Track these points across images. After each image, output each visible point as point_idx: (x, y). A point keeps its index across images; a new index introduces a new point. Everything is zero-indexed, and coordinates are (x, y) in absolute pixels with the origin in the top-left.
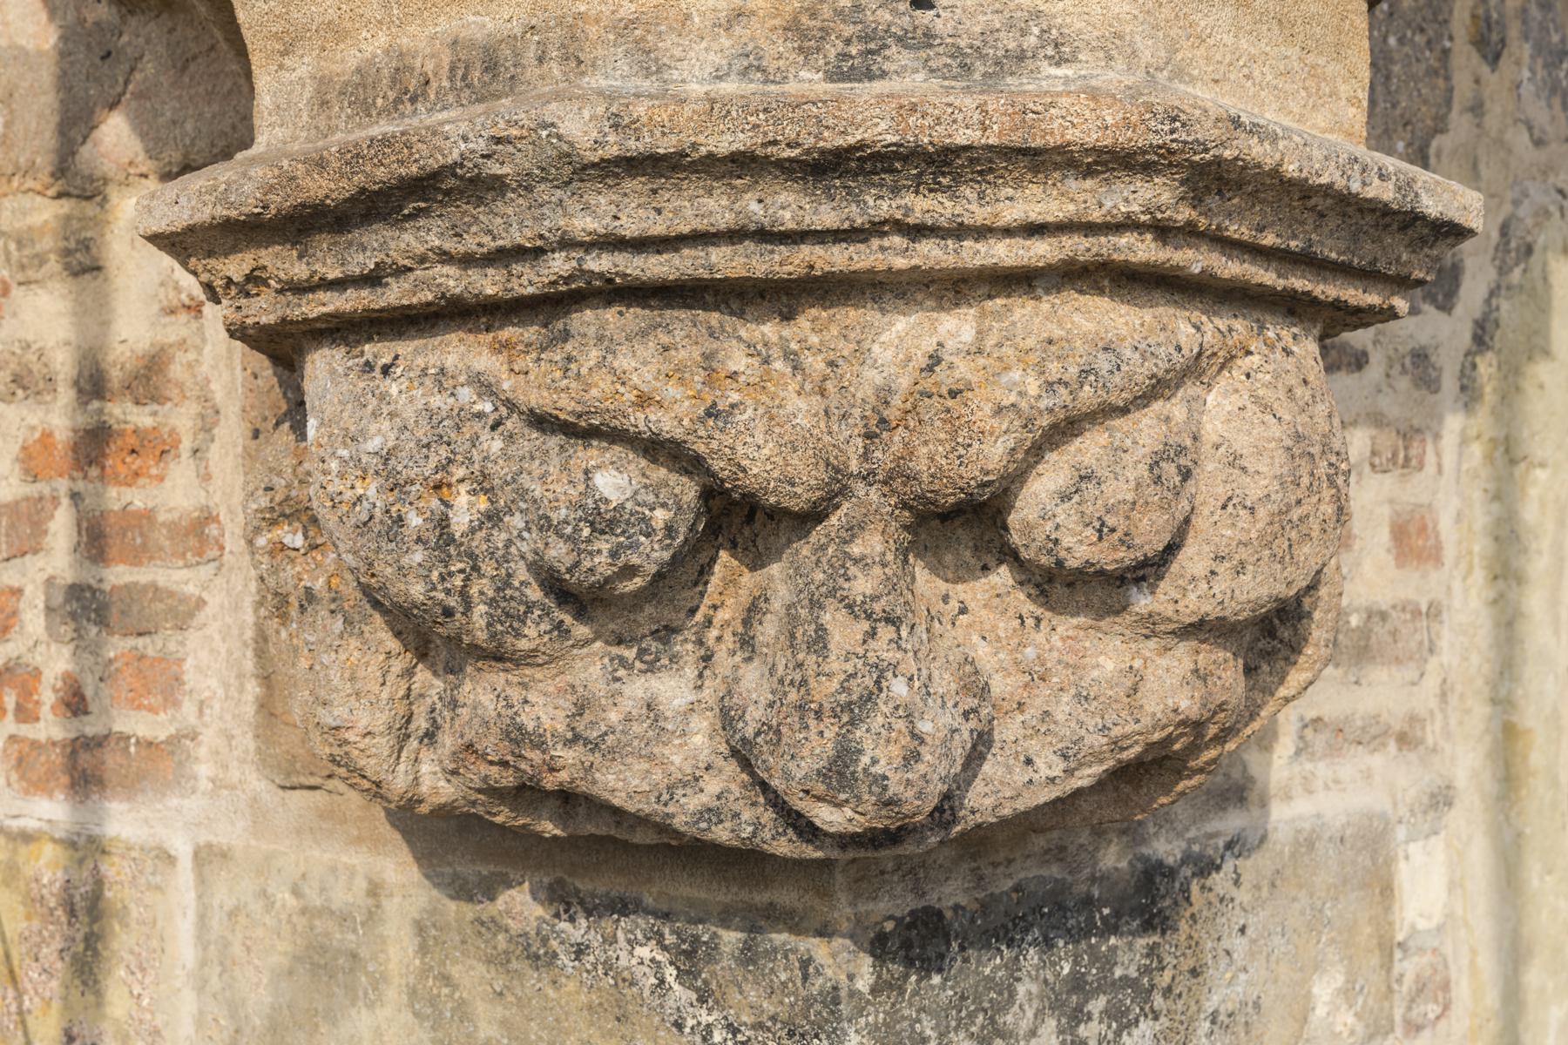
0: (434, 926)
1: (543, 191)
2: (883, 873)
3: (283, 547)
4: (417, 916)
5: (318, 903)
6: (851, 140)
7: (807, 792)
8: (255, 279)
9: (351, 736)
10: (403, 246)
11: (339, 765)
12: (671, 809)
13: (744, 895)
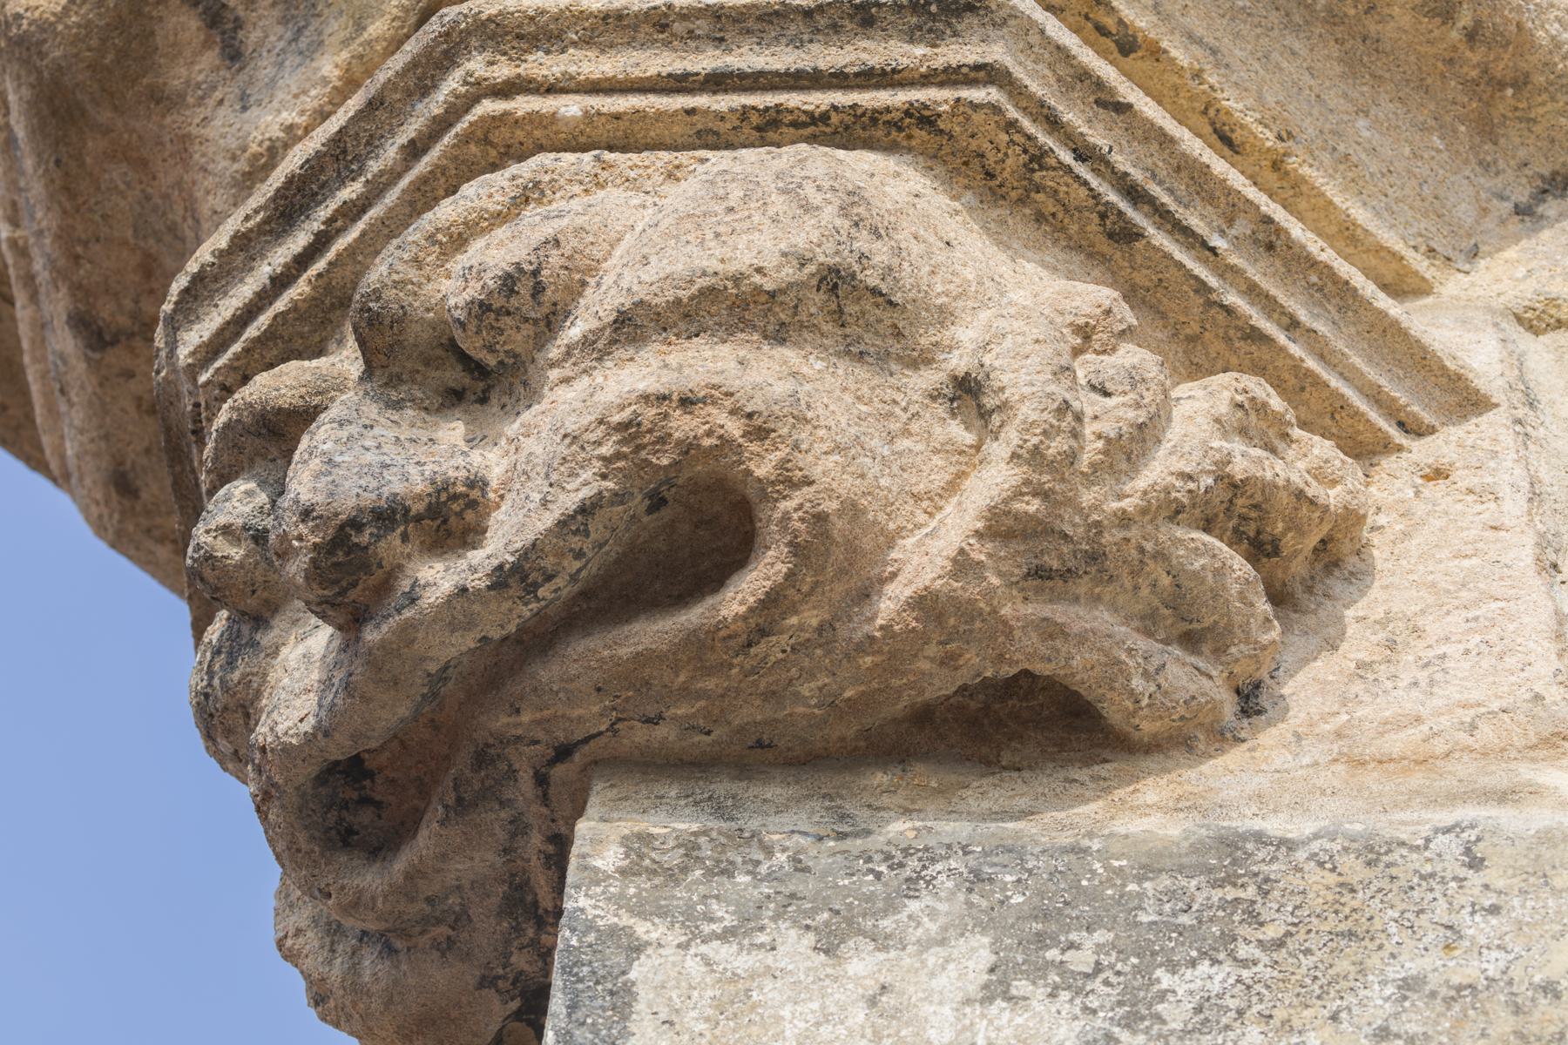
2: (662, 797)
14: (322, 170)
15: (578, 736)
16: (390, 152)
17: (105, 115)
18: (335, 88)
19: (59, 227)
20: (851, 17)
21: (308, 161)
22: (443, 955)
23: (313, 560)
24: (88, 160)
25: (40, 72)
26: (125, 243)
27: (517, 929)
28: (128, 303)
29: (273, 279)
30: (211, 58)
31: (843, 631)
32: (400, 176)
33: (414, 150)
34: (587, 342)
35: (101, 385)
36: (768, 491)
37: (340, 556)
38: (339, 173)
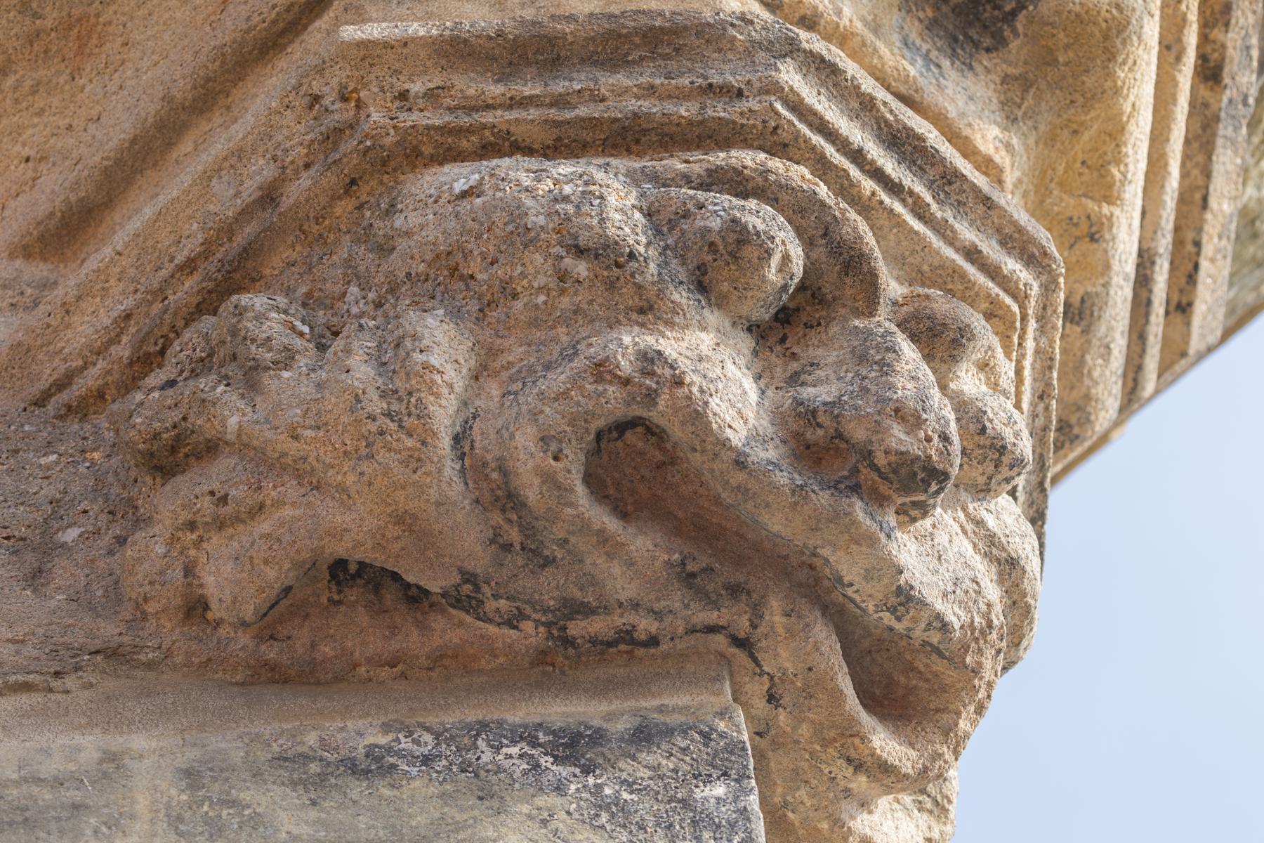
0: (211, 770)
1: (761, 55)
3: (293, 328)
4: (184, 766)
5: (15, 776)
6: (921, 131)
7: (897, 411)
8: (432, 96)
9: (438, 378)
10: (611, 81)
11: (393, 421)
12: (747, 450)
13: (632, 703)
14: (933, 165)
15: (759, 656)
16: (967, 234)
18: (838, 25)
20: (1037, 511)
21: (936, 150)
22: (492, 541)
23: (918, 458)
27: (545, 611)
29: (860, 151)
31: (845, 805)
32: (951, 244)
33: (972, 254)
34: (991, 539)
36: (947, 732)
37: (921, 475)
38: (935, 181)
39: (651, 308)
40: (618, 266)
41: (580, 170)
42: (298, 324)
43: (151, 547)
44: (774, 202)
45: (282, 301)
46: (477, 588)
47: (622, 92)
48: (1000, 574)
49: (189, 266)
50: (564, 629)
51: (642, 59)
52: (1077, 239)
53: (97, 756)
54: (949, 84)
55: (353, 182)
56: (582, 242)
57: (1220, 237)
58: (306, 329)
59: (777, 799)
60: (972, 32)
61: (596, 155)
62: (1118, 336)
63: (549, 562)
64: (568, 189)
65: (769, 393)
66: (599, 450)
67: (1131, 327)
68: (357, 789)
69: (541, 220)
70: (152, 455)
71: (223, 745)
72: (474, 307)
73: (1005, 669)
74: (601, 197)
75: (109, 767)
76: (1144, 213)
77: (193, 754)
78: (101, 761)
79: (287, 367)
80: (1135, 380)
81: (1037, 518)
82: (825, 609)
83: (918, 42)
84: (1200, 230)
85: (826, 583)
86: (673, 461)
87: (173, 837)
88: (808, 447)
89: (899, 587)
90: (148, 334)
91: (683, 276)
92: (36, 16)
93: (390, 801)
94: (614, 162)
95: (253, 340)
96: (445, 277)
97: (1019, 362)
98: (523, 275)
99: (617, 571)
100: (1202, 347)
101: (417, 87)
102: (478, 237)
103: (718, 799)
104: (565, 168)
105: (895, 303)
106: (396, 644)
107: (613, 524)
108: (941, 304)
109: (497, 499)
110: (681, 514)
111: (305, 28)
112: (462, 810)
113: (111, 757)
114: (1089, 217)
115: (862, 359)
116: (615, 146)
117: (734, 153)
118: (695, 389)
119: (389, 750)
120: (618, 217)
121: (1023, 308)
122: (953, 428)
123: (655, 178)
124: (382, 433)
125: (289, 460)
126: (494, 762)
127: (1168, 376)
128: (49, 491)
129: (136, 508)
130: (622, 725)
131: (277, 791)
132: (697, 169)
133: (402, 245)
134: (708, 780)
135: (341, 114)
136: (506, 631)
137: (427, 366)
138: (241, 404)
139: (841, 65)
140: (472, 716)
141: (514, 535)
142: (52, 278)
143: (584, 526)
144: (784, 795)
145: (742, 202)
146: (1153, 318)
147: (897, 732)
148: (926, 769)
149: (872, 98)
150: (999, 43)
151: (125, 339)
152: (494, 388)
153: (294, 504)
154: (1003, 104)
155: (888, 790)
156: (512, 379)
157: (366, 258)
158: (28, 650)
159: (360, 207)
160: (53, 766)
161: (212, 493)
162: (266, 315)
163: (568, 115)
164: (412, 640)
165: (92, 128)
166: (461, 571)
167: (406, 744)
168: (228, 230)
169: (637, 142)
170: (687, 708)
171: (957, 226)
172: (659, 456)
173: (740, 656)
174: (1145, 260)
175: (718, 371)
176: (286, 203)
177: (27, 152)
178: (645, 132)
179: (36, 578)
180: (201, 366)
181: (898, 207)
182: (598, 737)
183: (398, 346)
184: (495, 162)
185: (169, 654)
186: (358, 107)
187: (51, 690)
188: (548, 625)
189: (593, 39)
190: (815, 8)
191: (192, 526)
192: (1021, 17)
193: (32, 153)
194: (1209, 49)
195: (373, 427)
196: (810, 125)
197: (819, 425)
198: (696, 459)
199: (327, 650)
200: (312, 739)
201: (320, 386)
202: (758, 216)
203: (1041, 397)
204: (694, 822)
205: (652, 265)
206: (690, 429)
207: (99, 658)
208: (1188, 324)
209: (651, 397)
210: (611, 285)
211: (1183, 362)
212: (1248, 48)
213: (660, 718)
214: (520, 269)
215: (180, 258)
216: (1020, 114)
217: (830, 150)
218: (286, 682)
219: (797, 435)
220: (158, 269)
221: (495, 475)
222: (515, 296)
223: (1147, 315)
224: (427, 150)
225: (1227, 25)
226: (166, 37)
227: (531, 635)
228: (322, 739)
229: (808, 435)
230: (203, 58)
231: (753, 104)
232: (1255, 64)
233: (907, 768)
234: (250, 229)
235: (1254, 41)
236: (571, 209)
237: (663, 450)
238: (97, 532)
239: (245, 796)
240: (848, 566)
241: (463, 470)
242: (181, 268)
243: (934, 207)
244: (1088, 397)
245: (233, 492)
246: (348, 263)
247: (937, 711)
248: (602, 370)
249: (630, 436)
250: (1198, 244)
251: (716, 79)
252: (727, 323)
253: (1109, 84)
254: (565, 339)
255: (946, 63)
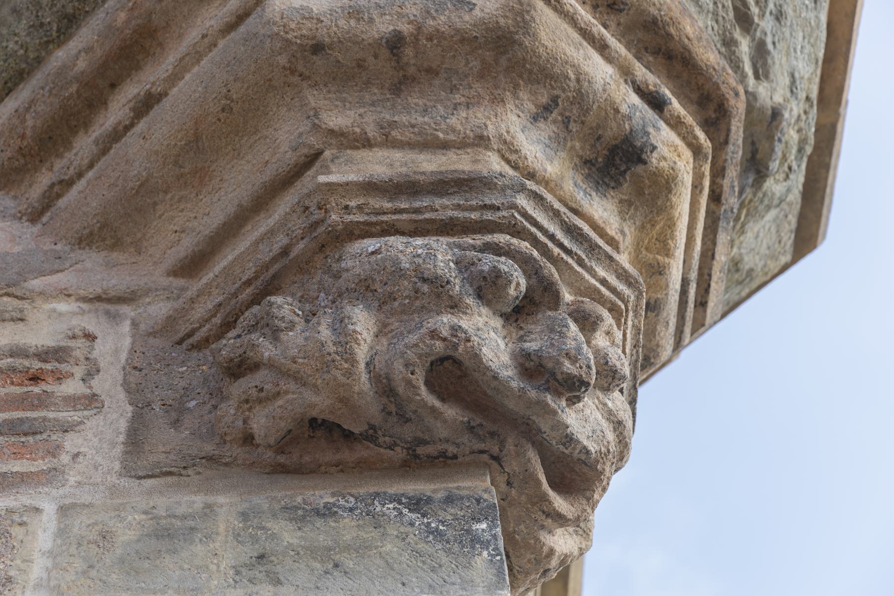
3: (295, 312)
5: (164, 514)
7: (567, 354)
8: (360, 208)
9: (359, 337)
13: (445, 485)
15: (503, 464)
16: (601, 272)
17: (503, 61)
19: (443, 32)
22: (383, 411)
23: (576, 376)
24: (480, 51)
25: (517, 33)
26: (442, 63)
28: (412, 61)
30: (534, 109)
32: (594, 277)
33: (604, 282)
35: (369, 44)
39: (456, 306)
40: (442, 287)
41: (426, 242)
42: (297, 310)
43: (228, 410)
44: (513, 258)
45: (290, 299)
46: (376, 432)
47: (445, 207)
48: (614, 428)
49: (248, 283)
50: (415, 450)
51: (455, 192)
52: (653, 274)
53: (202, 505)
54: (595, 203)
55: (323, 246)
56: (426, 276)
57: (720, 272)
58: (300, 313)
59: (511, 529)
60: (606, 180)
61: (433, 235)
62: (672, 317)
63: (408, 420)
64: (420, 251)
65: (510, 345)
66: (432, 370)
67: (678, 313)
68: (319, 522)
69: (407, 266)
70: (230, 368)
71: (259, 501)
72: (376, 304)
73: (616, 471)
74: (435, 256)
75: (208, 511)
76: (684, 262)
77: (246, 505)
78: (203, 509)
79: (291, 330)
80: (680, 338)
81: (633, 402)
82: (533, 443)
83: (581, 184)
84: (711, 269)
85: (534, 432)
86: (465, 375)
87: (236, 543)
88: (526, 370)
89: (567, 435)
90: (229, 313)
91: (471, 292)
92: (181, 167)
93: (334, 528)
94: (441, 239)
95: (276, 318)
96: (364, 289)
97: (624, 331)
98: (399, 290)
99: (439, 425)
100: (712, 322)
101: (353, 204)
102: (379, 272)
103: (483, 530)
104: (419, 241)
105: (568, 304)
106: (338, 457)
107: (437, 404)
108: (589, 305)
109: (385, 392)
110: (468, 399)
111: (303, 174)
112: (367, 533)
113: (208, 506)
114: (659, 264)
115: (552, 330)
116: (442, 232)
117: (495, 235)
118: (475, 343)
119: (334, 505)
120: (442, 264)
121: (626, 306)
122: (592, 362)
123: (459, 246)
124: (334, 361)
125: (291, 373)
126: (381, 511)
127: (696, 335)
128: (183, 384)
129: (222, 392)
130: (440, 495)
131: (283, 523)
132: (478, 243)
133: (345, 275)
134: (479, 521)
135: (318, 215)
136: (388, 451)
137: (354, 331)
138: (270, 347)
139: (545, 196)
140: (372, 490)
141: (393, 408)
142: (187, 285)
143: (424, 404)
144: (514, 527)
145: (499, 258)
146: (688, 309)
147: (565, 499)
148: (579, 516)
149: (559, 211)
150: (619, 184)
151: (218, 315)
152: (384, 341)
153: (293, 393)
154: (620, 212)
155: (561, 526)
156: (393, 337)
157: (328, 280)
158: (172, 457)
159: (326, 257)
160: (181, 510)
161: (256, 387)
162: (283, 305)
163: (421, 217)
164: (346, 455)
165: (205, 218)
166: (368, 424)
167: (342, 502)
168: (266, 267)
169: (452, 230)
170: (470, 488)
171: (597, 269)
172: (459, 373)
173: (495, 464)
174: (685, 283)
175: (486, 335)
176: (292, 255)
177: (176, 228)
178: (455, 225)
179: (176, 423)
180: (252, 329)
181: (570, 261)
182: (429, 500)
183: (341, 321)
184: (387, 238)
185: (236, 459)
186: (326, 212)
187: (181, 475)
188: (408, 449)
189: (432, 183)
190: (534, 169)
191: (247, 401)
192: (628, 173)
193: (178, 229)
194: (715, 187)
195: (329, 358)
196: (530, 223)
197: (532, 360)
198: (476, 374)
199: (307, 458)
200: (299, 499)
201: (306, 339)
202: (505, 265)
203: (635, 347)
204: (472, 540)
205: (457, 287)
206: (473, 361)
207: (204, 461)
208: (705, 311)
209: (455, 347)
210: (438, 296)
211: (703, 329)
212: (733, 187)
213: (457, 492)
214: (397, 287)
215: (244, 279)
216: (627, 217)
217: (539, 235)
218: (288, 473)
219: (521, 365)
220: (234, 284)
221: (384, 381)
222: (395, 300)
223: (686, 308)
224: (357, 232)
225: (724, 176)
226: (240, 177)
227: (399, 454)
228: (304, 499)
229: (526, 364)
230: (256, 188)
231: (505, 213)
232: (736, 194)
233: (570, 516)
234: (277, 267)
235: (736, 184)
236: (421, 261)
237: (461, 370)
238: (204, 403)
239: (269, 525)
240: (544, 425)
241: (370, 378)
242: (244, 283)
243: (587, 260)
244: (658, 346)
245: (266, 387)
246: (320, 282)
247: (584, 490)
248: (434, 334)
249: (446, 364)
250: (710, 275)
251: (488, 202)
252: (491, 313)
253: (668, 203)
254: (417, 319)
255: (594, 194)
